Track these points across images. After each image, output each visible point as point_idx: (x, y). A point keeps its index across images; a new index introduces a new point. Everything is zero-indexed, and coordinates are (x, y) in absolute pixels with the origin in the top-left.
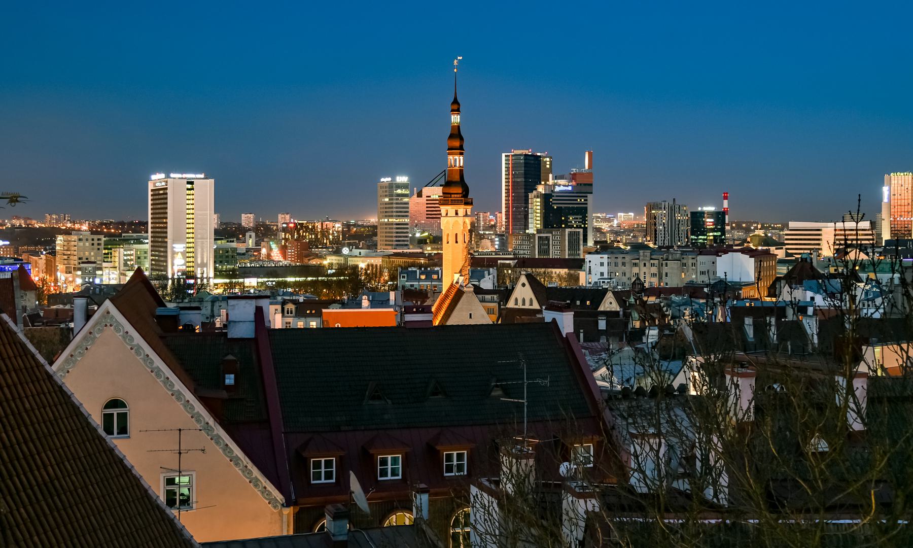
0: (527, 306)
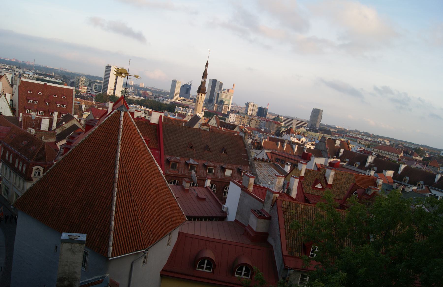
0: (214, 125)
